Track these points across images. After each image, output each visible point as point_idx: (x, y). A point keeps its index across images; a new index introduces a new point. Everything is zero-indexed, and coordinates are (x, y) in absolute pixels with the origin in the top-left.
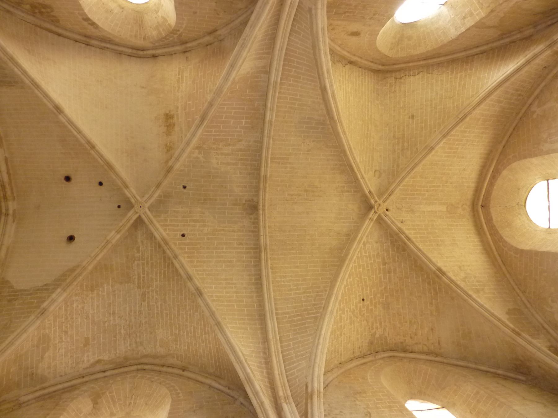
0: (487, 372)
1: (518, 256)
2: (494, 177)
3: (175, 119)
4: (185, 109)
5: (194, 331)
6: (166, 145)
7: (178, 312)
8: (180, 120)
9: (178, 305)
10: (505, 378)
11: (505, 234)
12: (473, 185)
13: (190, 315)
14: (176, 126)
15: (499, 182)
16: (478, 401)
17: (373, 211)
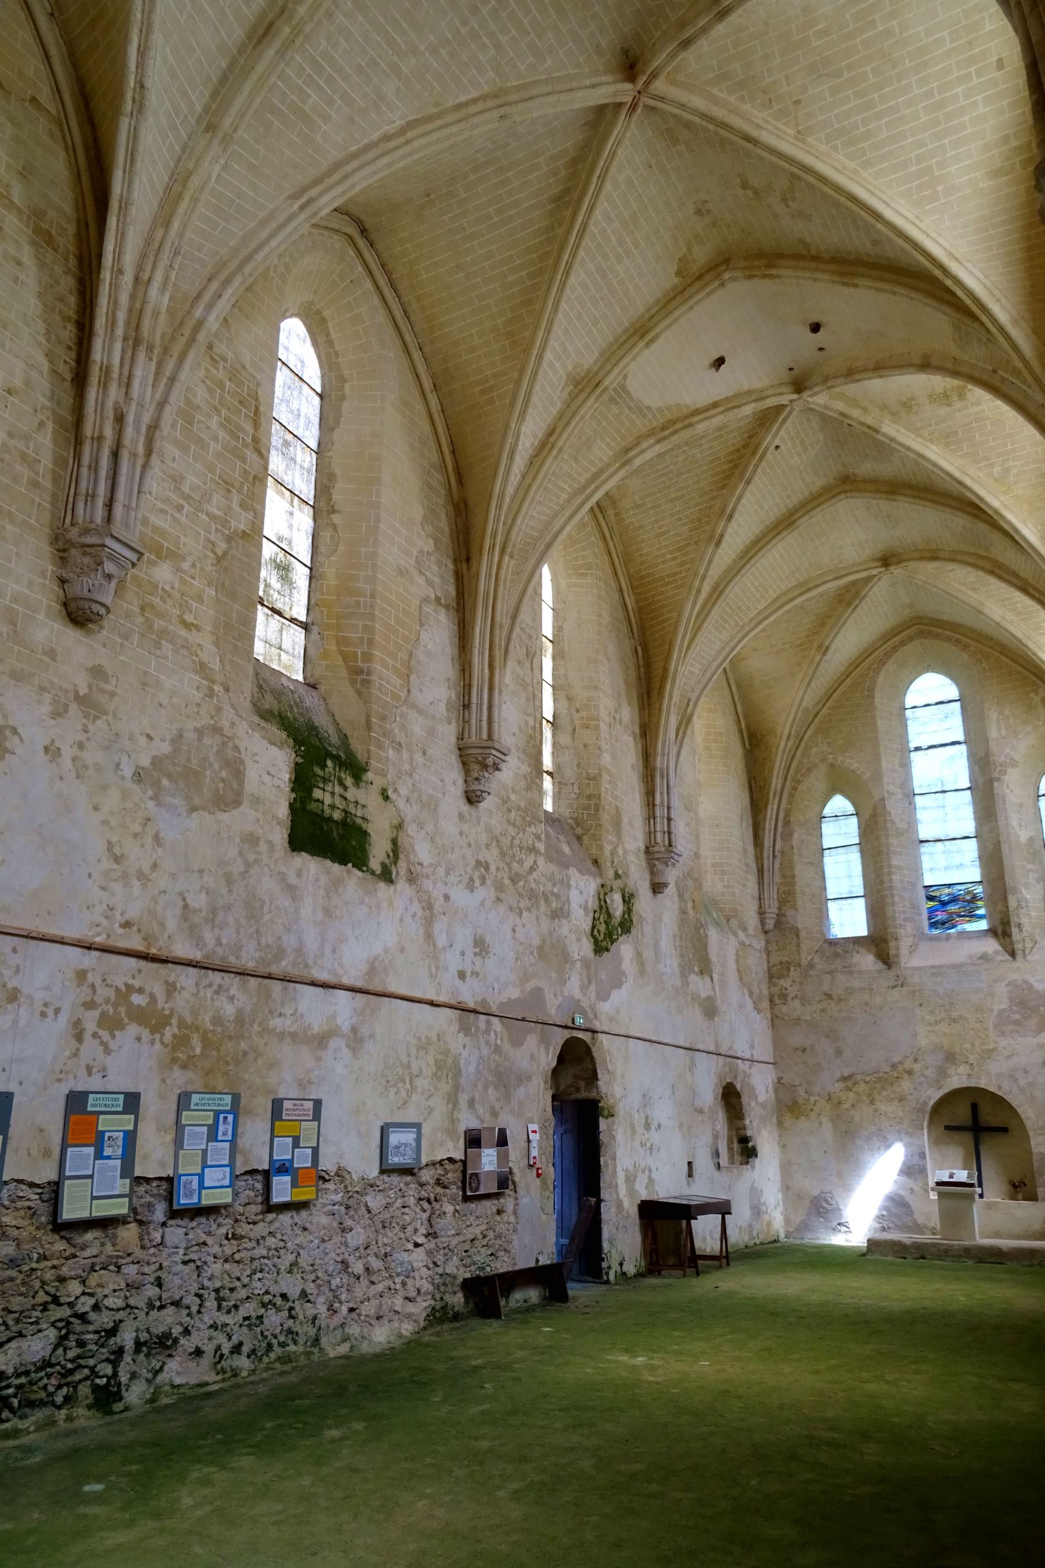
0: (737, 713)
1: (866, 693)
3: (959, 404)
6: (912, 398)
8: (958, 414)
9: (683, 496)
10: (741, 731)
13: (680, 519)
14: (947, 409)
16: (716, 741)
17: (883, 569)
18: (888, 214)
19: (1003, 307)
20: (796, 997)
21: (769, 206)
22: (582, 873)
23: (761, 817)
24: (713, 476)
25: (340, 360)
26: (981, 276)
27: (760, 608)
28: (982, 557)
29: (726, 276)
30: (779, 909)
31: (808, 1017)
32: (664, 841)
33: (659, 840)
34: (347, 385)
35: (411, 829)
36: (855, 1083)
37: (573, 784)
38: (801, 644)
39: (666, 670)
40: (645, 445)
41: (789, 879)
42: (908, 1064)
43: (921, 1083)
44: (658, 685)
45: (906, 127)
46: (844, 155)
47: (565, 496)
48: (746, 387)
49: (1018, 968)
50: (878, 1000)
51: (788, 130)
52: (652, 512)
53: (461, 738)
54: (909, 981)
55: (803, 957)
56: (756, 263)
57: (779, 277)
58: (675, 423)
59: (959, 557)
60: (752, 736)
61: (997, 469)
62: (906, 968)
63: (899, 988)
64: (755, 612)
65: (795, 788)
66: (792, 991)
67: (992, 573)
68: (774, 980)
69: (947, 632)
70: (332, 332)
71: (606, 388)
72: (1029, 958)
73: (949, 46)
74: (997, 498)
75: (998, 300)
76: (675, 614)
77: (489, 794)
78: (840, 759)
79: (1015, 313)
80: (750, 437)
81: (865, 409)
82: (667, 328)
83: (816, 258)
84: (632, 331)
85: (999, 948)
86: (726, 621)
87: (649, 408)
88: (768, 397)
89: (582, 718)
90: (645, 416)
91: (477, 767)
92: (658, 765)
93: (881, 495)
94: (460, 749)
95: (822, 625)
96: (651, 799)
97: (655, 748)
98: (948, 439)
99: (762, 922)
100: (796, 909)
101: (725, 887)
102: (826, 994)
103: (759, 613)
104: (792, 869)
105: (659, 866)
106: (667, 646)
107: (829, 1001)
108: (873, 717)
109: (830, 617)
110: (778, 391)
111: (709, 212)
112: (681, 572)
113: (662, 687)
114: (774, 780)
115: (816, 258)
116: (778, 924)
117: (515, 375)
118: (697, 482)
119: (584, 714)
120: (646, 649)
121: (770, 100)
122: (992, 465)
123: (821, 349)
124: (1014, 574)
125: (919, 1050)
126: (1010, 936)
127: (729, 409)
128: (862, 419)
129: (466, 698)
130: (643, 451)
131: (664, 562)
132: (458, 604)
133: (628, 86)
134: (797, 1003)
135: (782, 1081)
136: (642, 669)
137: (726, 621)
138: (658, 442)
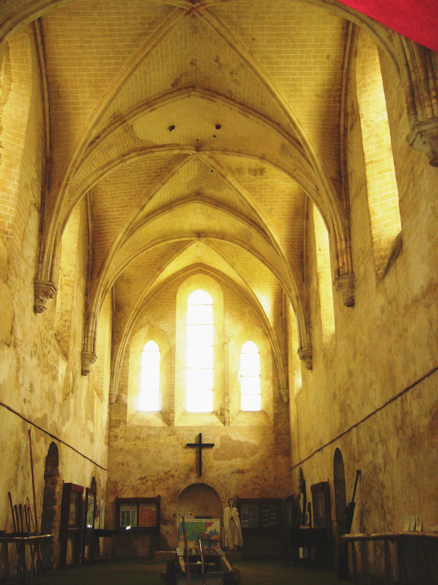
2: (216, 278)
3: (259, 177)
4: (265, 185)
5: (116, 197)
7: (126, 182)
11: (185, 283)
12: (213, 266)
13: (126, 193)
15: (214, 281)
17: (197, 238)
18: (279, 96)
19: (313, 148)
20: (122, 437)
21: (223, 73)
22: (63, 360)
23: (116, 346)
24: (146, 177)
25: (11, 70)
26: (307, 133)
27: (145, 244)
28: (245, 243)
29: (192, 93)
30: (119, 393)
31: (127, 448)
32: (91, 350)
33: (89, 350)
34: (13, 84)
35: (17, 319)
36: (147, 481)
37: (58, 313)
38: (151, 265)
39: (103, 264)
40: (132, 155)
41: (125, 378)
42: (172, 473)
43: (178, 482)
44: (97, 271)
45: (291, 66)
46: (266, 67)
47: (94, 169)
48: (177, 142)
49: (226, 430)
50: (162, 441)
51: (248, 49)
52: (112, 186)
53: (36, 278)
54: (177, 433)
55: (128, 418)
56: (207, 92)
57: (215, 102)
58: (146, 149)
59: (235, 241)
60: (117, 305)
61: (268, 207)
62: (176, 427)
63: (172, 436)
64: (142, 245)
65: (133, 334)
66: (120, 434)
67: (249, 250)
68: (112, 429)
69: (212, 273)
70: (10, 55)
71: (127, 125)
72: (230, 425)
73: (313, 43)
74: (266, 219)
75: (312, 145)
76: (113, 238)
77: (46, 309)
78: (157, 323)
79: (317, 151)
80: (169, 164)
81: (222, 167)
82: (162, 106)
83: (234, 100)
84: (145, 102)
85: (218, 420)
86: (130, 247)
87: (138, 138)
88: (185, 149)
89: (66, 280)
90: (135, 141)
91: (43, 294)
92: (93, 310)
93: (212, 205)
94: (35, 283)
95: (163, 258)
96: (87, 327)
97: (93, 302)
98: (251, 189)
99: (110, 399)
100: (127, 394)
101: (99, 378)
102: (137, 437)
103: (144, 246)
104: (128, 374)
105: (87, 362)
106: (106, 253)
107: (139, 441)
108: (175, 306)
109: (167, 255)
110: (189, 148)
111: (196, 65)
112: (120, 218)
113: (100, 272)
114: (126, 329)
115: (234, 100)
116: (117, 400)
117: (96, 106)
118: (139, 178)
119: (67, 278)
120: (93, 252)
121: (243, 34)
122: (266, 205)
123: (214, 136)
124: (258, 253)
125: (178, 465)
126: (224, 415)
127: (169, 150)
128: (220, 171)
129: (41, 258)
130: (130, 158)
131: (112, 211)
132: (41, 208)
133: (191, 4)
134: (122, 440)
135: (110, 479)
136: (91, 262)
137: (130, 247)
138: (138, 155)
